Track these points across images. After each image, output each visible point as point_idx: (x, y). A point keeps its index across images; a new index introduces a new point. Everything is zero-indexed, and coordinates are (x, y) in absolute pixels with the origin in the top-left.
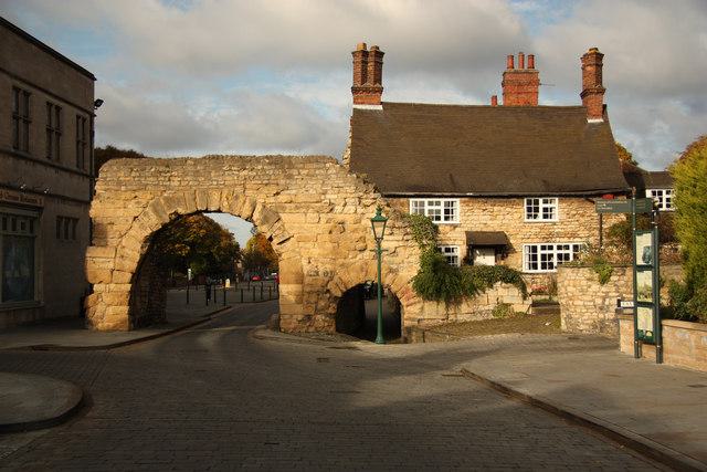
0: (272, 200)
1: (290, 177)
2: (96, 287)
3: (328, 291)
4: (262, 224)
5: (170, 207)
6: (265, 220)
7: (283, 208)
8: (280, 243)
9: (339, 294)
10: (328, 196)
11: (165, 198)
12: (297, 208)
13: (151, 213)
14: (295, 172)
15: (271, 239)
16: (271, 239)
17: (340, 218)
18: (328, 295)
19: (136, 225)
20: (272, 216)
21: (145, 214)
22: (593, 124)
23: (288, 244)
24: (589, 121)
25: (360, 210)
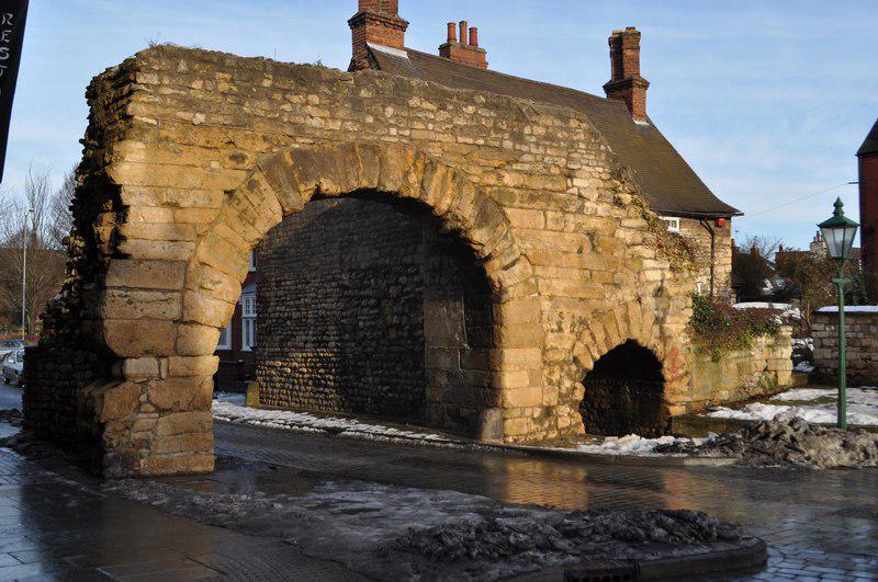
0: (492, 180)
1: (518, 138)
2: (132, 367)
3: (576, 360)
4: (479, 226)
5: (305, 178)
6: (484, 218)
7: (512, 197)
8: (506, 268)
9: (590, 365)
10: (577, 182)
11: (296, 154)
12: (533, 198)
13: (264, 184)
14: (527, 130)
15: (489, 258)
16: (489, 258)
17: (593, 223)
18: (574, 368)
19: (233, 212)
20: (491, 208)
21: (252, 185)
22: (639, 126)
23: (517, 268)
24: (637, 122)
25: (617, 212)
